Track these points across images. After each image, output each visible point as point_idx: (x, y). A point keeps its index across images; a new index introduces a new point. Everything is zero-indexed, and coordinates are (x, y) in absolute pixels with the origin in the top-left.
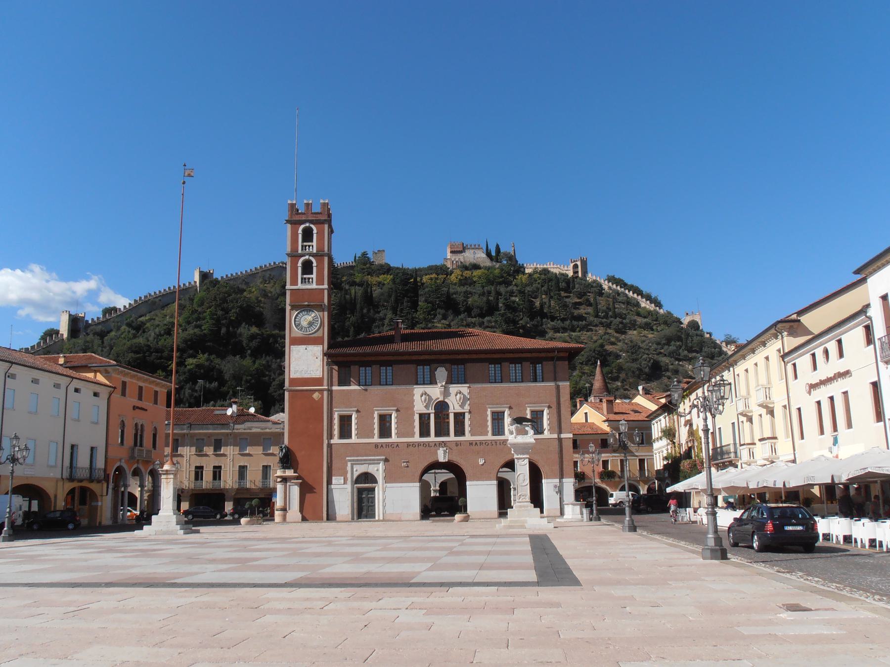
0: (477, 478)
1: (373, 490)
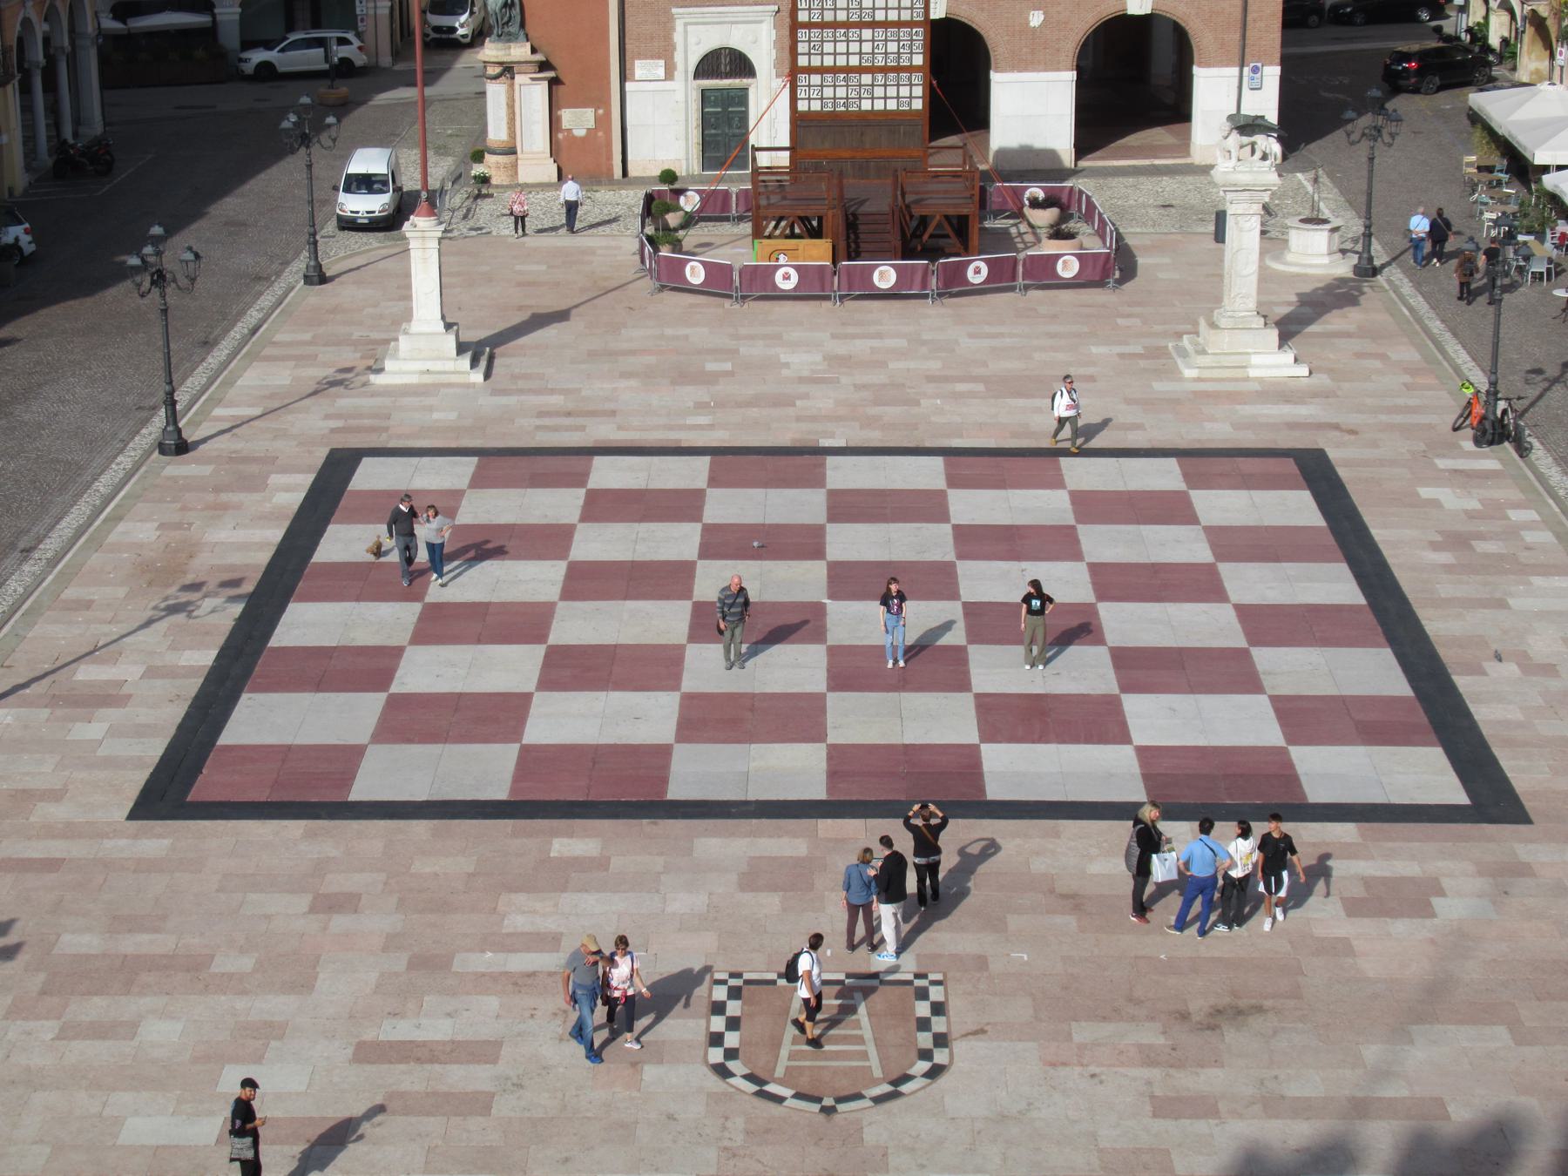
0: (1021, 64)
1: (741, 97)
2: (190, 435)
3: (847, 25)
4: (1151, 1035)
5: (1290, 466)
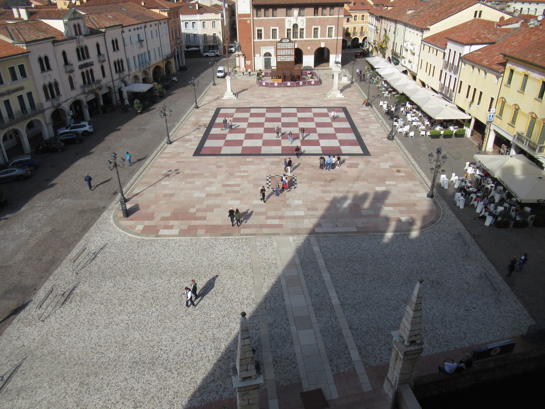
0: (307, 54)
1: (270, 59)
2: (199, 106)
3: (284, 49)
4: (322, 183)
5: (341, 109)
